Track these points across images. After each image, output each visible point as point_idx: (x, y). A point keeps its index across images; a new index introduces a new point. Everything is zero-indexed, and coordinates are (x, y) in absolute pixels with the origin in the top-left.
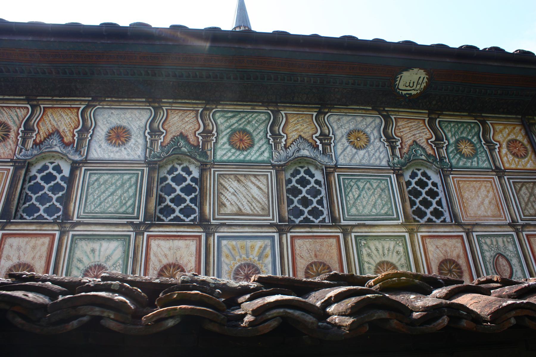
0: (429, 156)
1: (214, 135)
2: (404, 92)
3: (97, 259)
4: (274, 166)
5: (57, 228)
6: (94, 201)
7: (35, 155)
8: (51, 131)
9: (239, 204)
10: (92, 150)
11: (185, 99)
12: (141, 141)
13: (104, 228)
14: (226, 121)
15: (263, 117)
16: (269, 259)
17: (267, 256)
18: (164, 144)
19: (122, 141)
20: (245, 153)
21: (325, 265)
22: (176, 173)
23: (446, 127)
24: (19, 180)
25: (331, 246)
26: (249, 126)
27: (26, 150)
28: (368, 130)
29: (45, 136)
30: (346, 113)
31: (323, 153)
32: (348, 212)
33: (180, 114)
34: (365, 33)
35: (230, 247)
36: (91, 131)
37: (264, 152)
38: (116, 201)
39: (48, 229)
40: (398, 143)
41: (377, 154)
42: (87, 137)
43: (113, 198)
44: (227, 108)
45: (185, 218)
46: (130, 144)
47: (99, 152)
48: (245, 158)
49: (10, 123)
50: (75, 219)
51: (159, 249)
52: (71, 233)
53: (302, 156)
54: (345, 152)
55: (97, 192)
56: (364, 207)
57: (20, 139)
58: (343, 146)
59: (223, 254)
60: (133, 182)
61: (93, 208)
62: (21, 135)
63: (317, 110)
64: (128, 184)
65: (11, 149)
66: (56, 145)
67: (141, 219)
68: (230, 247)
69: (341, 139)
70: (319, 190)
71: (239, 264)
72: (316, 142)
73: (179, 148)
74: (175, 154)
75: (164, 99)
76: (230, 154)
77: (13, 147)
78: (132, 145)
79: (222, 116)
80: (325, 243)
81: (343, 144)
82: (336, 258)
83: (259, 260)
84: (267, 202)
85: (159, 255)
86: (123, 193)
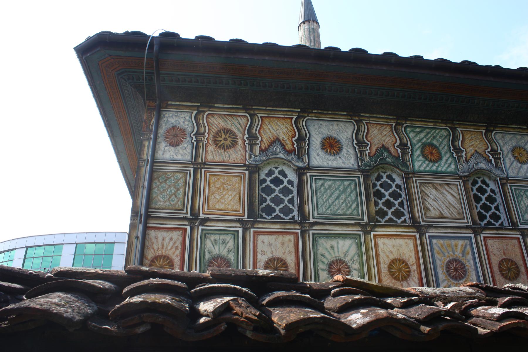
1: (409, 148)
3: (337, 255)
4: (461, 177)
5: (298, 227)
6: (324, 204)
7: (264, 161)
8: (273, 140)
9: (440, 209)
10: (312, 158)
11: (379, 114)
12: (351, 151)
13: (337, 228)
14: (416, 136)
15: (445, 133)
16: (470, 256)
17: (468, 254)
19: (335, 151)
20: (437, 165)
21: (512, 261)
22: (382, 180)
24: (255, 183)
25: (515, 246)
26: (435, 140)
30: (508, 131)
31: (496, 167)
32: (523, 218)
33: (378, 128)
35: (440, 245)
36: (307, 140)
38: (342, 204)
39: (291, 228)
42: (305, 146)
43: (339, 202)
44: (415, 124)
45: (397, 220)
46: (343, 153)
47: (318, 160)
48: (437, 169)
49: (235, 130)
50: (311, 219)
51: (385, 247)
53: (481, 169)
54: (512, 166)
55: (325, 196)
57: (247, 145)
58: (510, 161)
59: (435, 251)
60: (353, 188)
61: (324, 210)
62: (247, 142)
63: (485, 128)
64: (349, 190)
65: (242, 155)
66: (280, 152)
67: (366, 221)
68: (440, 245)
70: (495, 198)
71: (448, 259)
72: (489, 157)
73: (385, 159)
74: (381, 164)
75: (362, 113)
76: (425, 165)
77: (243, 152)
78: (345, 155)
79: (412, 131)
80: (510, 244)
81: (510, 159)
82: (519, 256)
83: (463, 256)
84: (460, 208)
85: (386, 251)
86: (347, 198)
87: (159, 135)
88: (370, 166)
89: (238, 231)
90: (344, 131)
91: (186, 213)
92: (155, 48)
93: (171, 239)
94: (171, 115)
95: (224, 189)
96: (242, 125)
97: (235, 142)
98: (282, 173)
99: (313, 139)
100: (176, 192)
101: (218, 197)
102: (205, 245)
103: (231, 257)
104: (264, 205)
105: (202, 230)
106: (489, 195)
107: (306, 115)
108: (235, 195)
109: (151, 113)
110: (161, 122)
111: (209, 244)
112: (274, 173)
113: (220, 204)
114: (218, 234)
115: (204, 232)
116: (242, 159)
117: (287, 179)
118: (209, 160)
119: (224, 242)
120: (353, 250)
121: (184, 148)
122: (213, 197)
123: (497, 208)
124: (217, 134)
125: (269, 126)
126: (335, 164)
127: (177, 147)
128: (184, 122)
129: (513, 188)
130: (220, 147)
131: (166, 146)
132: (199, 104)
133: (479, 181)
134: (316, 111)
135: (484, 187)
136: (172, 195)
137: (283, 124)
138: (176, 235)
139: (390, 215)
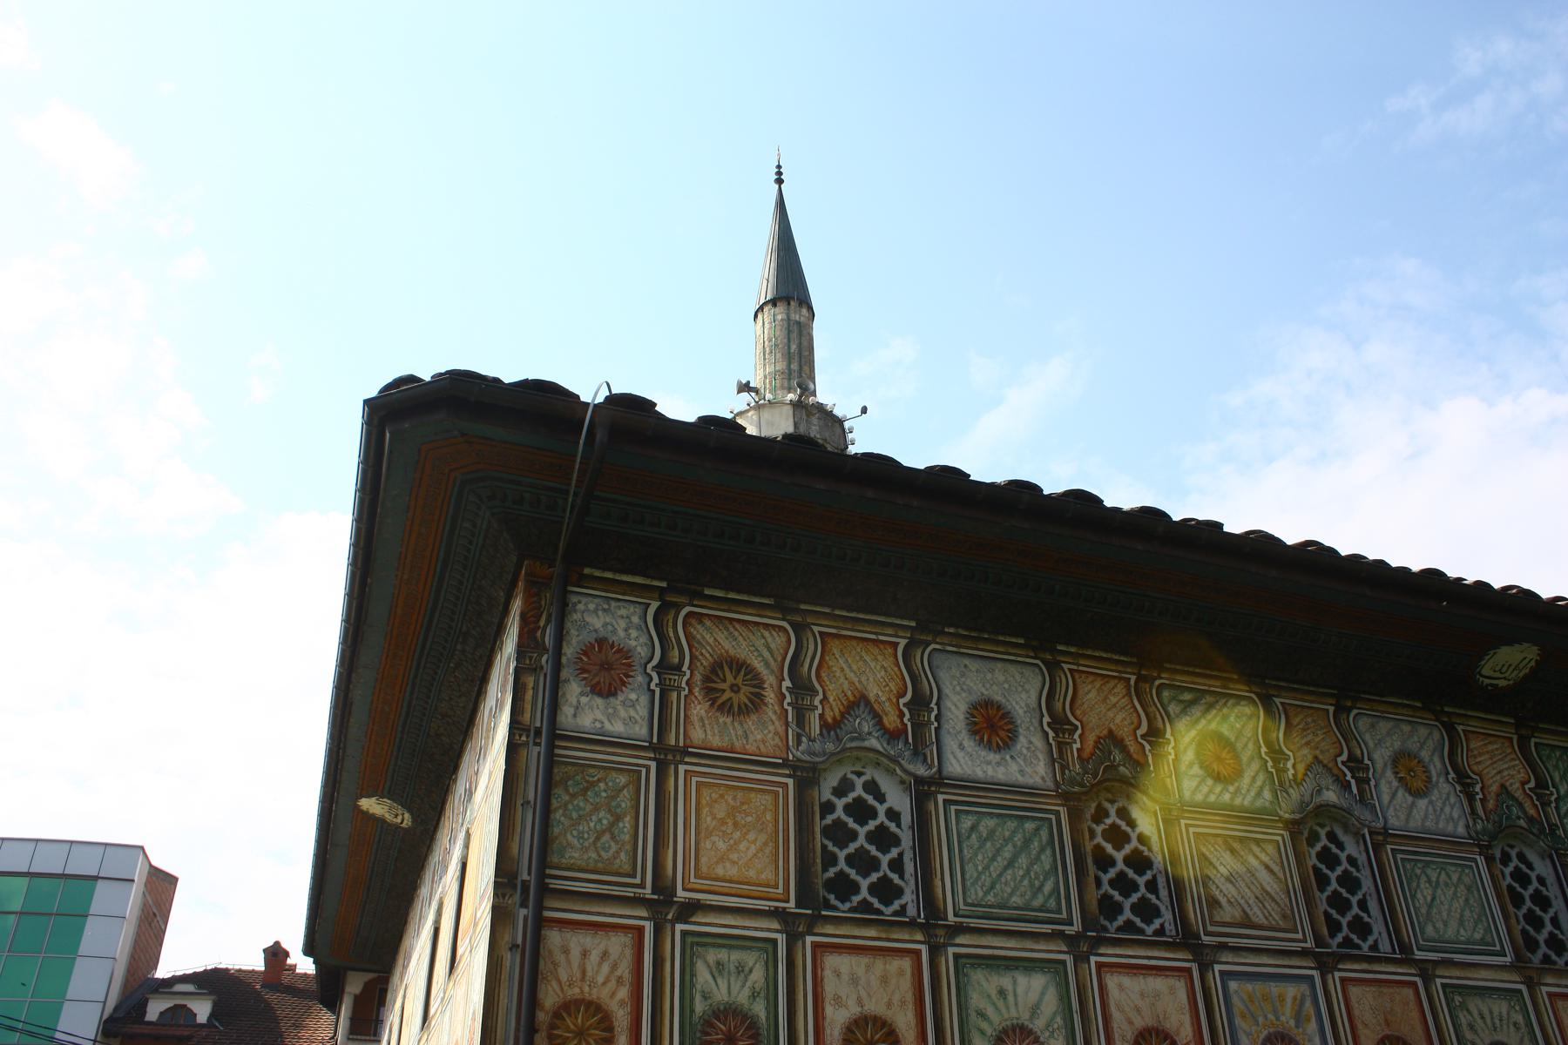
0: (1530, 820)
2: (1487, 681)
3: (1014, 1013)
5: (919, 937)
6: (978, 878)
7: (832, 754)
10: (948, 756)
12: (1038, 742)
13: (1012, 943)
16: (1312, 1026)
17: (1309, 1020)
18: (1085, 755)
20: (1231, 789)
22: (1108, 821)
23: (1549, 757)
27: (810, 740)
28: (1425, 754)
32: (1422, 933)
33: (1098, 684)
34: (1464, 567)
37: (1261, 788)
40: (1478, 788)
41: (1447, 809)
42: (929, 722)
44: (1181, 680)
48: (1232, 799)
49: (758, 665)
52: (951, 950)
56: (1445, 924)
59: (1236, 1011)
61: (981, 894)
62: (788, 699)
65: (776, 733)
67: (1077, 927)
69: (1384, 771)
71: (1265, 1033)
73: (1113, 767)
76: (1205, 789)
79: (1173, 699)
86: (1032, 864)
87: (564, 660)
88: (1082, 785)
89: (774, 941)
90: (1019, 689)
91: (642, 886)
92: (600, 436)
93: (605, 955)
94: (592, 607)
95: (736, 825)
97: (759, 696)
98: (871, 787)
100: (612, 825)
101: (721, 845)
102: (693, 975)
103: (759, 1009)
104: (831, 872)
105: (684, 933)
106: (1345, 871)
107: (930, 638)
108: (765, 844)
110: (568, 625)
111: (703, 975)
112: (852, 787)
113: (728, 865)
114: (723, 946)
115: (689, 940)
117: (886, 806)
118: (696, 742)
119: (740, 969)
120: (1051, 1003)
122: (708, 845)
123: (1363, 905)
124: (713, 671)
126: (1000, 774)
127: (612, 699)
129: (1399, 856)
130: (721, 708)
132: (664, 584)
133: (1323, 833)
134: (952, 630)
135: (1334, 849)
136: (603, 832)
137: (876, 659)
138: (618, 945)
139: (1127, 914)
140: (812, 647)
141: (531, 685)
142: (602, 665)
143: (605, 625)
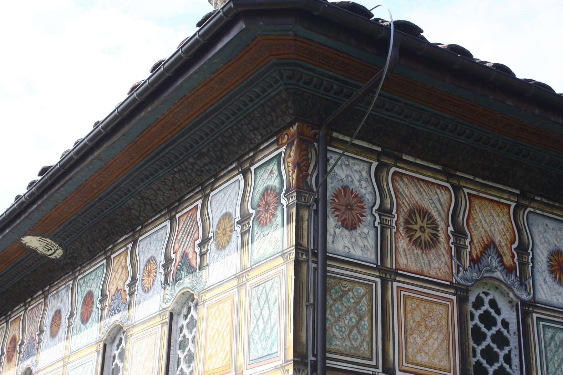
7: (477, 281)
10: (538, 287)
27: (465, 270)
29: (481, 250)
36: (529, 251)
49: (435, 214)
55: (556, 358)
57: (453, 246)
62: (452, 240)
65: (446, 264)
77: (447, 258)
91: (376, 367)
95: (426, 326)
96: (444, 206)
98: (493, 304)
99: (537, 250)
100: (358, 322)
101: (419, 341)
108: (443, 341)
109: (306, 149)
113: (423, 354)
116: (446, 272)
118: (402, 267)
121: (363, 236)
122: (412, 341)
124: (410, 216)
125: (480, 215)
127: (353, 232)
128: (359, 181)
130: (415, 243)
131: (336, 227)
132: (379, 149)
134: (539, 199)
137: (499, 216)
140: (463, 203)
141: (306, 218)
142: (347, 206)
143: (347, 176)
